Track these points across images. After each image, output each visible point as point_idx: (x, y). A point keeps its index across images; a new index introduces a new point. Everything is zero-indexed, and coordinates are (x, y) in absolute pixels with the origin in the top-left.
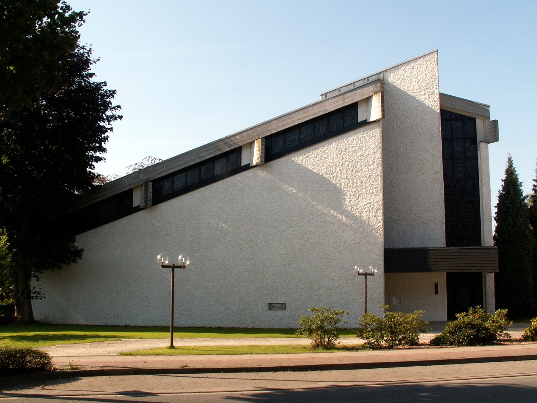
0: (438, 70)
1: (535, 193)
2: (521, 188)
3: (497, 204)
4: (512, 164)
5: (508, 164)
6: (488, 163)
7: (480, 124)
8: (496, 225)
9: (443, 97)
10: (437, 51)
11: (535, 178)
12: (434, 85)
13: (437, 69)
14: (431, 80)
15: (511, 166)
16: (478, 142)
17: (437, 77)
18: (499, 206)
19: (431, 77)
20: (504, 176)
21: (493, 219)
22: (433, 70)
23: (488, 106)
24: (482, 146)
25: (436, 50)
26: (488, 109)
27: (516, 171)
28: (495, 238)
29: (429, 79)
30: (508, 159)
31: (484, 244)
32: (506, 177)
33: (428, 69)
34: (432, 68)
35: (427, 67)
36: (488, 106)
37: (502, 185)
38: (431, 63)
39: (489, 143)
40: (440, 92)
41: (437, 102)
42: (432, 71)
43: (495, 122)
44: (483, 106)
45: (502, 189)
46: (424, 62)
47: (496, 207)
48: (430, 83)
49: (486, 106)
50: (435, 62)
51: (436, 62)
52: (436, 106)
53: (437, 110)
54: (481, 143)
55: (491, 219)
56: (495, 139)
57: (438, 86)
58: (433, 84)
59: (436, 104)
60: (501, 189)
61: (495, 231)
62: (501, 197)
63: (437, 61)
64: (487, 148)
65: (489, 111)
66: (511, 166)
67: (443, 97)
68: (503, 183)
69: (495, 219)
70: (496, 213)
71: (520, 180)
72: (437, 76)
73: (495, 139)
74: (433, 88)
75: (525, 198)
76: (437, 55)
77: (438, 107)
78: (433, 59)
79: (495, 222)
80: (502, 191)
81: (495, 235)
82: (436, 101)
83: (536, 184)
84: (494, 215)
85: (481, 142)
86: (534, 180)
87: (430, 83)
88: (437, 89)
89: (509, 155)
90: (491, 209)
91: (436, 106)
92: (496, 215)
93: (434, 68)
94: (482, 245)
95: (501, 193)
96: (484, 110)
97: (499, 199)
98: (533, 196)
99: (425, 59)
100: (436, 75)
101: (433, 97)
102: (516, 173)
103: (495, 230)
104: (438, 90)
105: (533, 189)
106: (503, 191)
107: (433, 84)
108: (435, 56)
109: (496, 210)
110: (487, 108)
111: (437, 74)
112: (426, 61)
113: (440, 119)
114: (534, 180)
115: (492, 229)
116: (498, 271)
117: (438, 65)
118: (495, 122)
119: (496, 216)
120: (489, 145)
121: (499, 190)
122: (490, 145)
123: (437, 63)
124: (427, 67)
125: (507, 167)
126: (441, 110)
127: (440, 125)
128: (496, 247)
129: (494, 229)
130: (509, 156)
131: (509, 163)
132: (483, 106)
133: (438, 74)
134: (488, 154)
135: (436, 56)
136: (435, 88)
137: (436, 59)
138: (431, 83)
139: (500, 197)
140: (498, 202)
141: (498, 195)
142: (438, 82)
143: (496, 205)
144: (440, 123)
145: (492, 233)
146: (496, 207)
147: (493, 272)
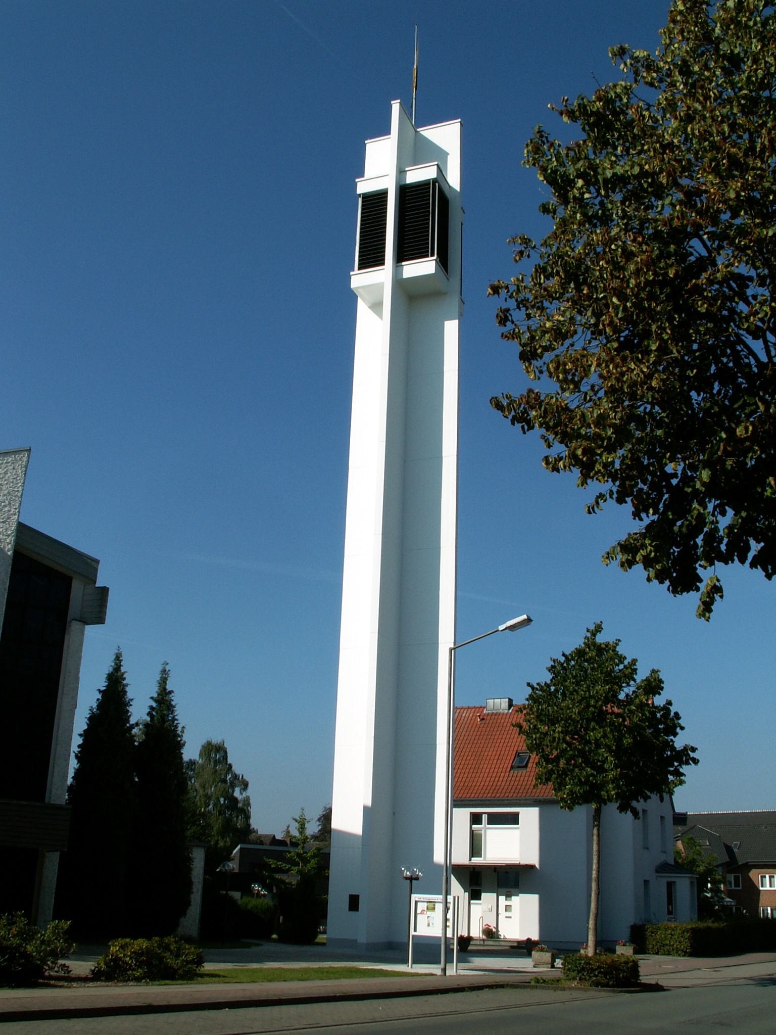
0: (24, 483)
1: (151, 721)
2: (130, 709)
3: (85, 731)
4: (121, 666)
5: (113, 664)
6: (80, 658)
7: (77, 587)
8: (77, 766)
9: (23, 530)
10: (30, 450)
11: (155, 695)
12: (10, 507)
13: (22, 481)
14: (9, 498)
15: (117, 667)
16: (68, 620)
17: (19, 494)
18: (86, 735)
19: (8, 492)
20: (102, 684)
21: (73, 755)
22: (15, 481)
23: (97, 562)
24: (75, 626)
25: (28, 448)
26: (95, 566)
27: (124, 679)
28: (70, 789)
29: (4, 495)
30: (115, 656)
31: (50, 798)
32: (107, 686)
33: (7, 478)
34: (15, 477)
35: (6, 473)
36: (97, 562)
37: (98, 700)
38: (14, 469)
39: (88, 624)
40: (20, 520)
41: (10, 537)
42: (13, 482)
43: (104, 591)
44: (89, 561)
45: (97, 706)
46: (2, 463)
47: (80, 735)
48: (5, 502)
49: (94, 561)
50: (21, 468)
51: (24, 469)
52: (8, 544)
53: (8, 551)
54: (74, 621)
55: (69, 756)
56: (99, 619)
57: (17, 510)
58: (10, 504)
59: (8, 541)
60: (95, 705)
61: (73, 777)
62: (93, 720)
63: (26, 468)
64: (82, 632)
65: (97, 569)
66: (117, 667)
67: (23, 530)
68: (100, 697)
69: (77, 756)
70: (79, 746)
71: (130, 695)
72: (20, 493)
73: (99, 619)
74: (9, 511)
75: (132, 727)
76: (29, 456)
77: (10, 546)
78: (20, 462)
79: (76, 761)
80: (95, 710)
81: (71, 785)
82: (9, 535)
83: (154, 705)
84: (75, 748)
85: (73, 619)
86: (152, 698)
87: (5, 502)
88: (15, 514)
89: (119, 650)
90: (71, 739)
91: (8, 544)
92: (80, 750)
93: (18, 478)
94: (47, 801)
95: (93, 713)
96: (89, 566)
97: (88, 722)
98: (146, 725)
99: (6, 459)
100: (18, 491)
101: (5, 528)
102: (124, 682)
103: (73, 775)
104: (17, 516)
105: (149, 714)
106: (97, 709)
107: (10, 504)
108: (24, 458)
109: (80, 741)
110: (93, 564)
111: (20, 489)
112: (6, 462)
113: (10, 567)
114: (152, 698)
115: (67, 773)
116: (66, 850)
117: (25, 474)
118: (104, 591)
119: (79, 752)
120: (87, 627)
121: (92, 707)
122: (88, 628)
123: (26, 471)
124: (6, 473)
125: (111, 669)
126: (16, 552)
127: (9, 578)
128: (70, 807)
129: (71, 773)
130: (117, 652)
131: (116, 664)
132: (89, 561)
133: (23, 490)
134: (82, 642)
135: (25, 459)
136: (12, 512)
137: (24, 463)
138: (7, 502)
139: (90, 719)
140: (86, 727)
141: (88, 716)
142: (20, 504)
143: (82, 733)
144: (9, 575)
145: (67, 780)
146: (80, 735)
147: (56, 851)
